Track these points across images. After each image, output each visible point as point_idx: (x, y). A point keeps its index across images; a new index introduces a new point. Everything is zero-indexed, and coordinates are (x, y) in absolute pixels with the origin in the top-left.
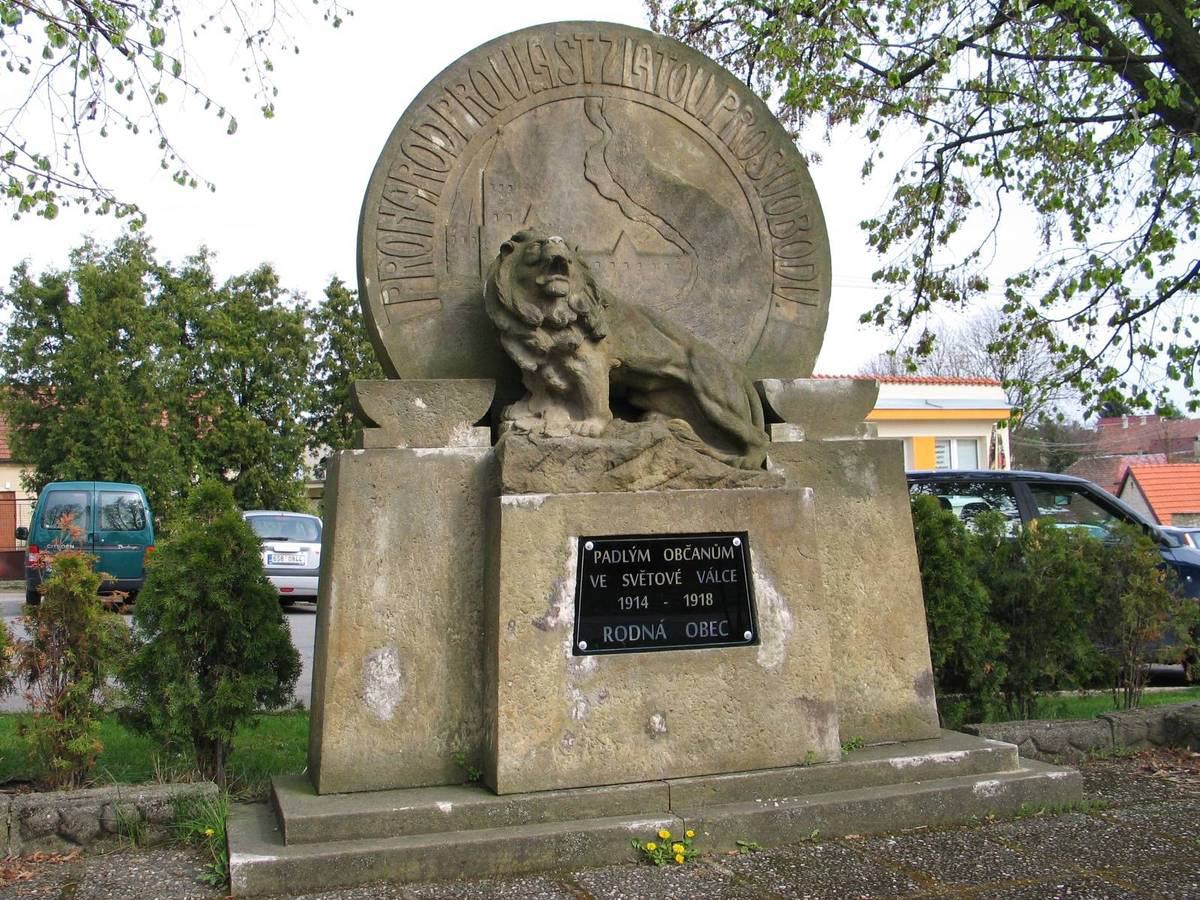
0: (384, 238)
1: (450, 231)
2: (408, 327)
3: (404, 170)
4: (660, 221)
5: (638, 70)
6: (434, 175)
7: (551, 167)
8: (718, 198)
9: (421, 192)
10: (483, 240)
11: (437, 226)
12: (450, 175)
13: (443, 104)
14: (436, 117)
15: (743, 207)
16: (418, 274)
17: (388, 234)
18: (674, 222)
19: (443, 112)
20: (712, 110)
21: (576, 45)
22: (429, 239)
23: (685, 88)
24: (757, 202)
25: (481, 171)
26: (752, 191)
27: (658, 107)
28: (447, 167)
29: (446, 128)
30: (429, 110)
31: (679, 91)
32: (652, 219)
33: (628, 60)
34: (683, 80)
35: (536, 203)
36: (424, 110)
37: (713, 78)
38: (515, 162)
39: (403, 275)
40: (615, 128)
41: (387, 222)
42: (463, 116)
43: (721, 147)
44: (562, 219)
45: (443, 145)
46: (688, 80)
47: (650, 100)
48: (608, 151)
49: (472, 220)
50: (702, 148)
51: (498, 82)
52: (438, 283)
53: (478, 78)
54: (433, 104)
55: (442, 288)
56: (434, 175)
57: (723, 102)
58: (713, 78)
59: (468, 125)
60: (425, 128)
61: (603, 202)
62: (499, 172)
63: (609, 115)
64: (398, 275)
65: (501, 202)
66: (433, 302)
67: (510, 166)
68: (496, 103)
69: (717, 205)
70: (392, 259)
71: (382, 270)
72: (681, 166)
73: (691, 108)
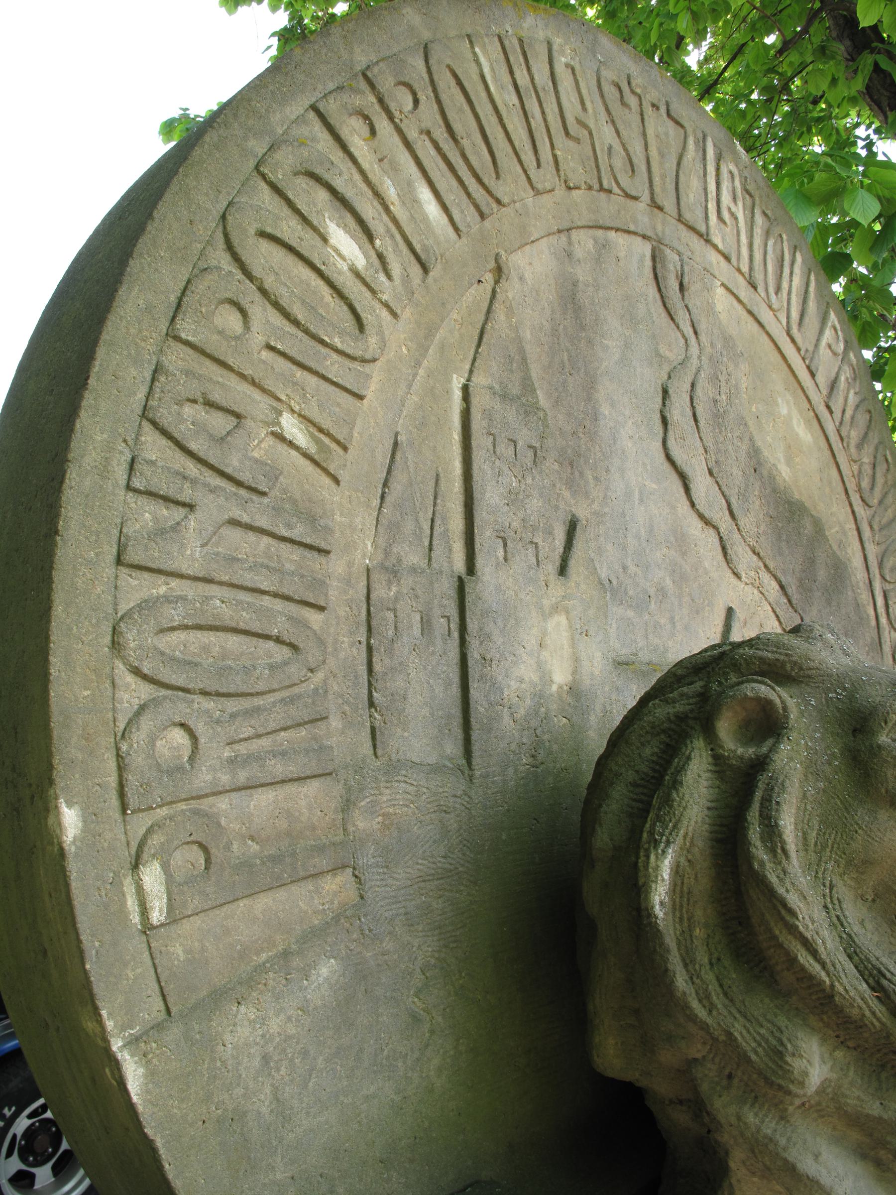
0: (147, 606)
1: (381, 592)
2: (247, 1012)
3: (232, 320)
4: (772, 587)
5: (726, 215)
6: (333, 366)
7: (605, 410)
8: (832, 533)
9: (290, 425)
10: (472, 625)
11: (336, 565)
12: (376, 372)
13: (357, 123)
14: (337, 156)
15: (857, 562)
16: (278, 768)
17: (161, 587)
18: (792, 590)
19: (359, 145)
20: (817, 346)
21: (632, 101)
22: (314, 618)
23: (785, 285)
24: (872, 551)
25: (457, 383)
26: (867, 533)
27: (755, 311)
28: (373, 340)
29: (369, 210)
30: (317, 127)
31: (778, 290)
32: (766, 578)
33: (712, 186)
34: (782, 266)
35: (582, 512)
36: (300, 120)
37: (812, 277)
38: (535, 372)
39: (225, 779)
40: (703, 338)
41: (161, 532)
42: (410, 184)
43: (831, 429)
44: (632, 569)
45: (361, 262)
46: (786, 270)
47: (744, 292)
48: (699, 391)
49: (438, 551)
50: (807, 422)
51: (494, 119)
52: (347, 806)
53: (445, 82)
54: (331, 107)
55: (362, 823)
56: (333, 366)
57: (828, 334)
58: (812, 277)
59: (425, 219)
60: (303, 182)
61: (695, 527)
62: (504, 397)
63: (694, 301)
64: (203, 778)
65: (513, 498)
66: (331, 884)
67: (528, 386)
68: (489, 178)
69: (834, 553)
70: (179, 709)
71: (137, 760)
72: (789, 461)
73: (795, 331)
